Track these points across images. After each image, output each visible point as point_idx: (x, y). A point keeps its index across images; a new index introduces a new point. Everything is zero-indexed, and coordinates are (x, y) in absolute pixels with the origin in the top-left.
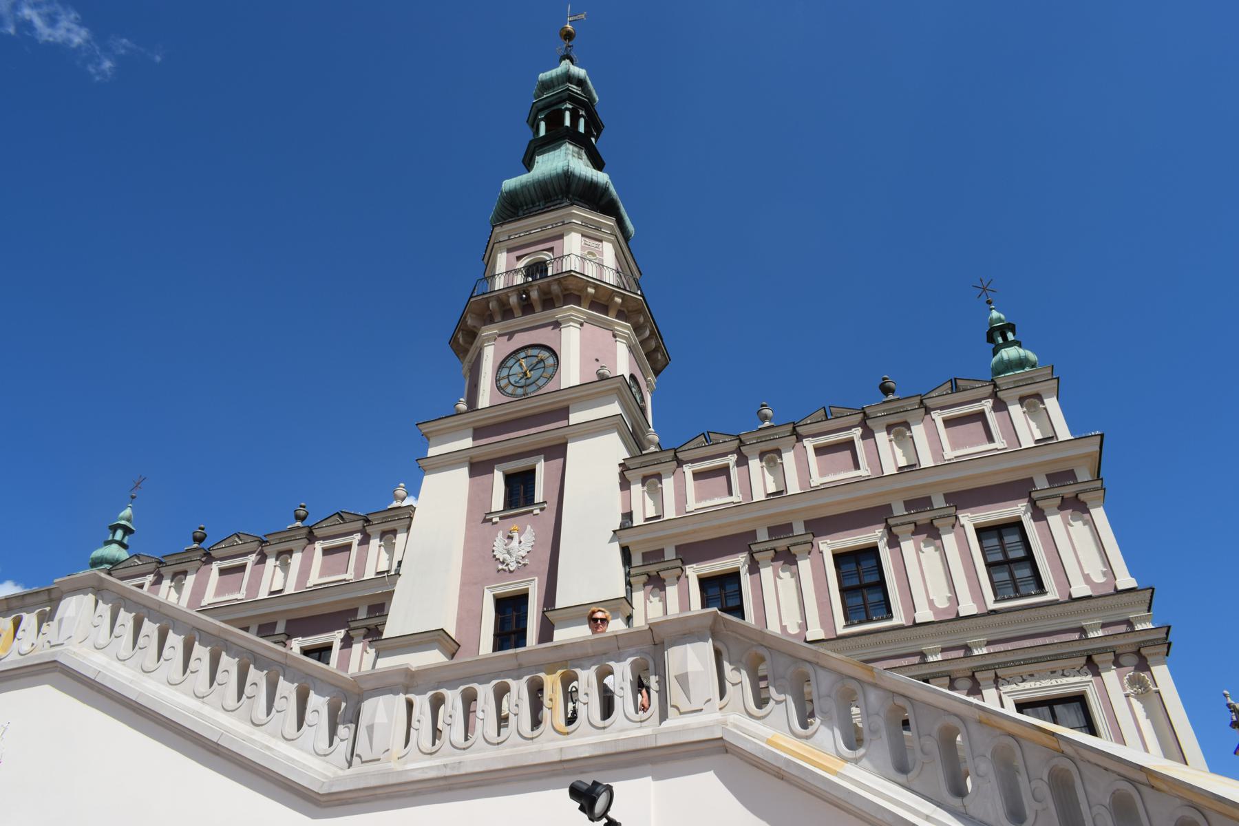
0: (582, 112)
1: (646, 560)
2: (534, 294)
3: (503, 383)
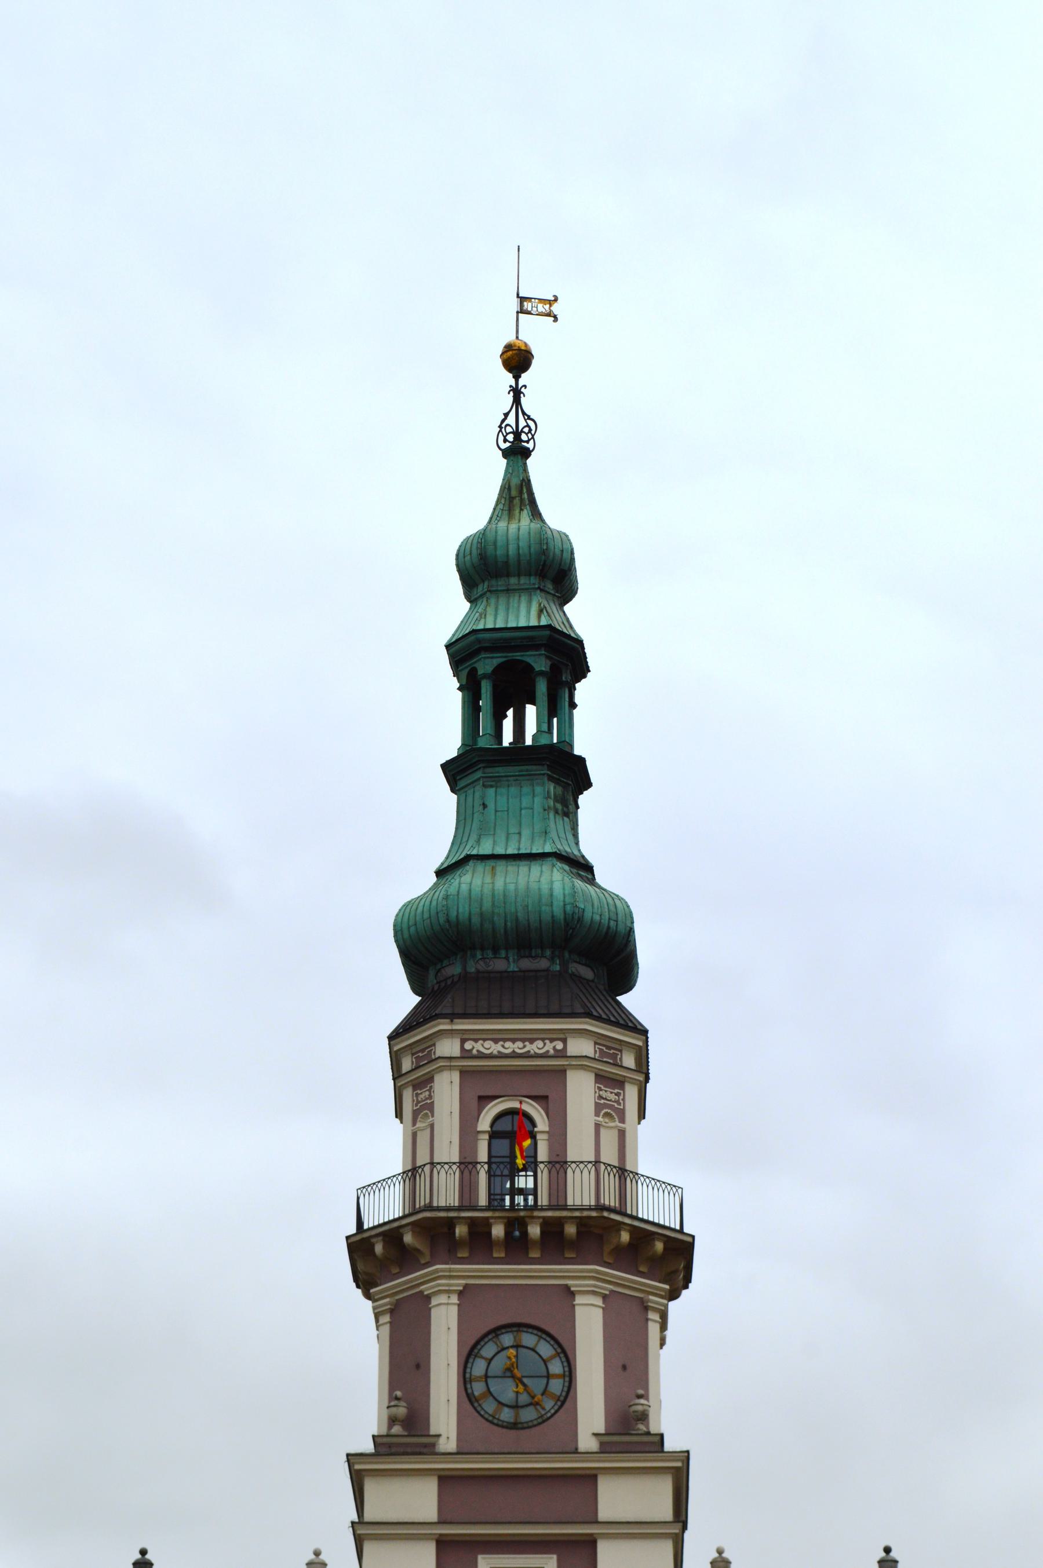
2: (534, 1231)
3: (478, 1388)
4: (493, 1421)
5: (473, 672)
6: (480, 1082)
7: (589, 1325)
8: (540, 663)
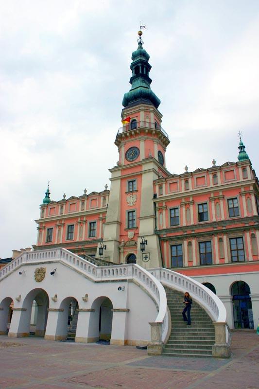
0: (145, 66)
2: (133, 133)
8: (139, 65)
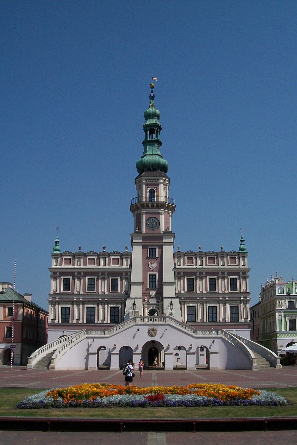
1: (179, 275)
2: (155, 205)
4: (149, 229)
5: (146, 130)
6: (147, 185)
7: (162, 217)
